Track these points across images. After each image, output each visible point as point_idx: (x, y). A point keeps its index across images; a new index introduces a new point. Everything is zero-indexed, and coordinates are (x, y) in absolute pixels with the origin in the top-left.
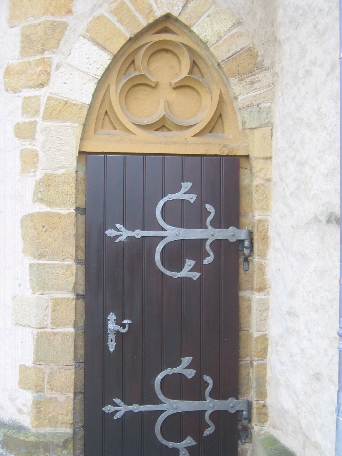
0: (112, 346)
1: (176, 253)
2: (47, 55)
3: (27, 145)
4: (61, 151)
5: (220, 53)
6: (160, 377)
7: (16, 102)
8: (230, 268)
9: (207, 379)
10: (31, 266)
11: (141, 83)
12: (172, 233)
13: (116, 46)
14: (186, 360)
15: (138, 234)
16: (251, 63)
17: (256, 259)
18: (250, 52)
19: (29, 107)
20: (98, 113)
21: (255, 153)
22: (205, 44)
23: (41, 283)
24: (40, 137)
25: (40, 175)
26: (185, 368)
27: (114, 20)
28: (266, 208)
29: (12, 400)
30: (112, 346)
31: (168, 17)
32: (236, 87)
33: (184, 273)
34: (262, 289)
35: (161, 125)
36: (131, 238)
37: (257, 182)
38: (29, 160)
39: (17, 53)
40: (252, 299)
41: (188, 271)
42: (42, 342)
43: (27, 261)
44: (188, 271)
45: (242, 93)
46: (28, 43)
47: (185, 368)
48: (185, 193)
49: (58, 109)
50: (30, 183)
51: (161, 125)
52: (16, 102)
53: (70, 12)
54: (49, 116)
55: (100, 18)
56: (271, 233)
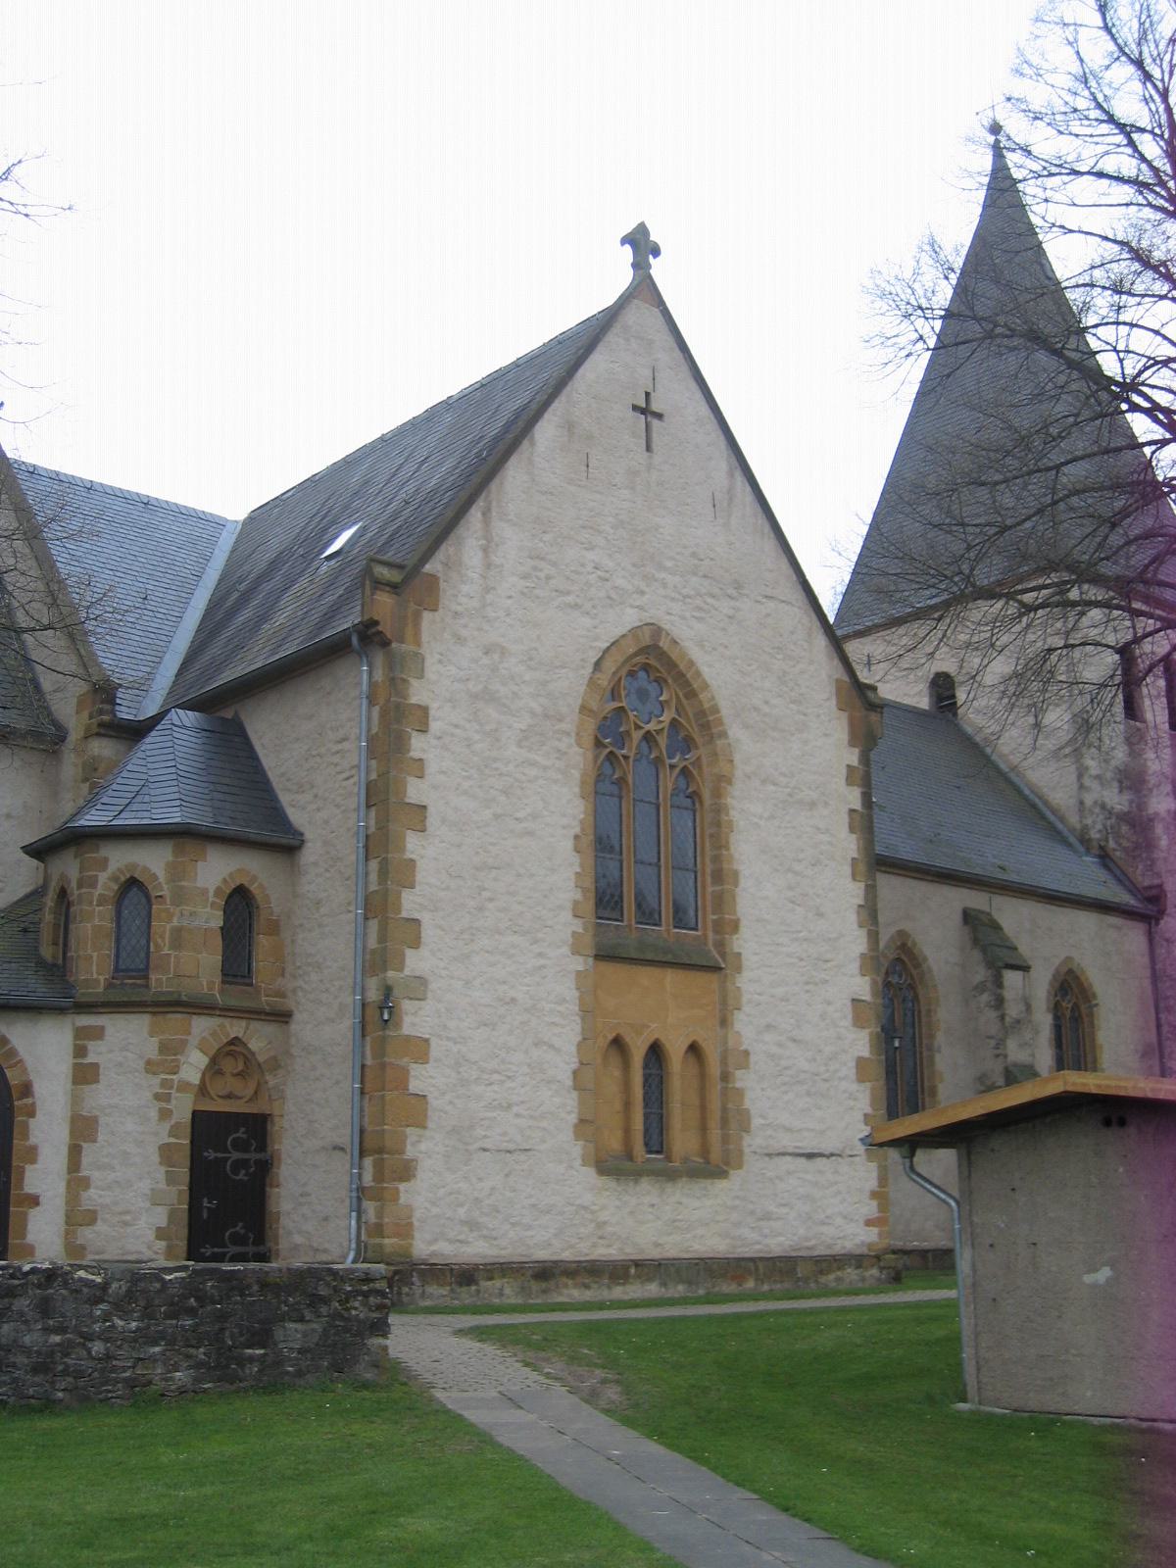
0: (205, 1215)
1: (239, 1165)
2: (179, 1057)
3: (164, 1105)
4: (183, 1107)
5: (261, 1059)
6: (227, 1234)
7: (156, 1080)
8: (263, 1172)
9: (251, 1235)
10: (167, 1172)
11: (220, 1073)
12: (236, 1155)
13: (212, 1052)
14: (241, 1224)
15: (220, 1155)
16: (275, 1064)
17: (275, 1170)
18: (275, 1058)
19: (164, 1084)
20: (202, 1090)
21: (276, 1112)
22: (253, 1054)
23: (171, 1180)
24: (174, 1102)
25: (173, 1122)
26: (239, 1228)
27: (211, 1040)
28: (280, 1143)
29: (149, 1248)
30: (205, 1215)
31: (236, 1038)
32: (268, 1077)
33: (240, 1177)
34: (277, 1186)
35: (229, 1096)
36: (216, 1158)
37: (276, 1128)
38: (164, 1114)
39: (156, 1052)
40: (272, 1192)
41: (242, 1176)
42: (172, 1215)
43: (163, 1169)
44: (242, 1176)
45: (272, 1081)
46: (164, 1048)
47: (239, 1228)
48: (241, 1134)
49: (184, 1086)
50: (167, 1126)
51: (229, 1096)
52: (156, 1080)
53: (190, 1034)
54: (178, 1090)
55: (204, 1038)
56: (283, 1156)
